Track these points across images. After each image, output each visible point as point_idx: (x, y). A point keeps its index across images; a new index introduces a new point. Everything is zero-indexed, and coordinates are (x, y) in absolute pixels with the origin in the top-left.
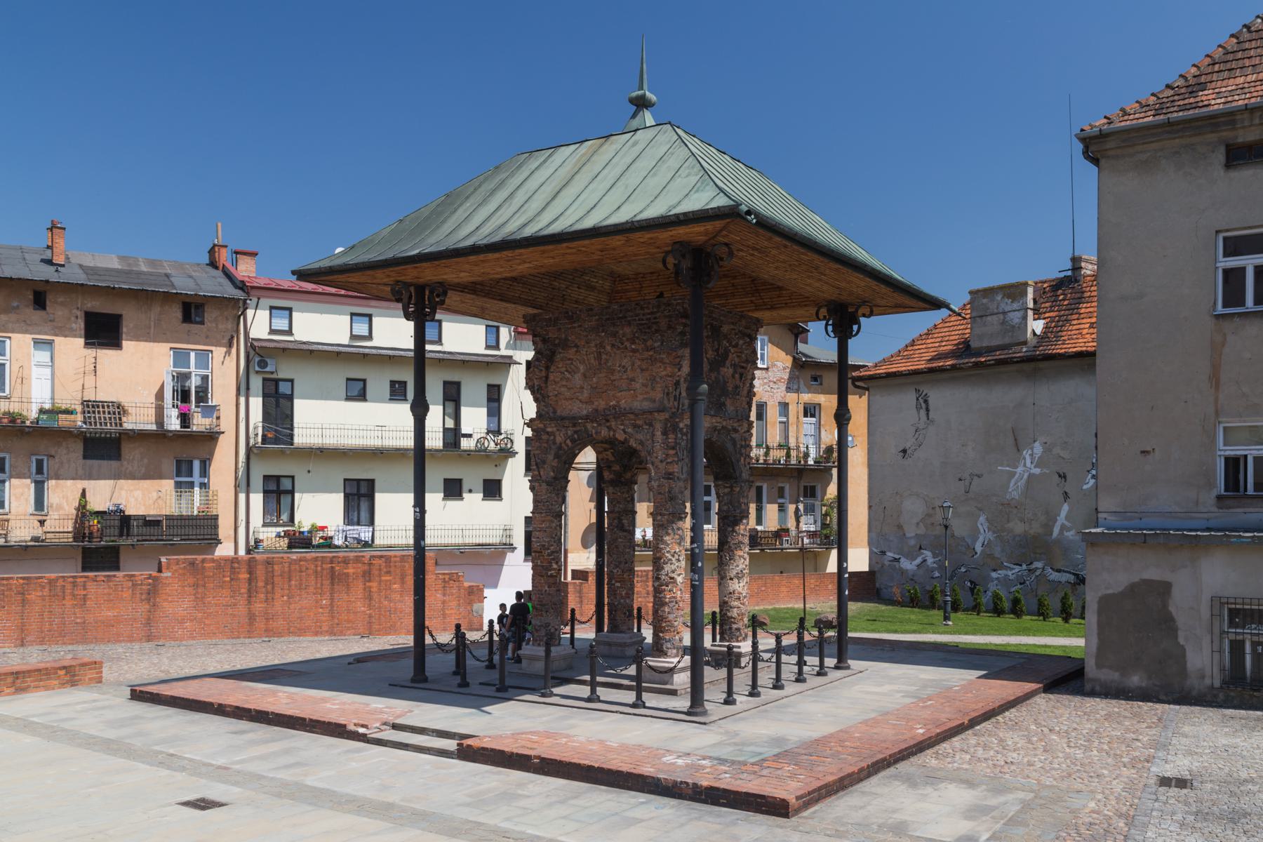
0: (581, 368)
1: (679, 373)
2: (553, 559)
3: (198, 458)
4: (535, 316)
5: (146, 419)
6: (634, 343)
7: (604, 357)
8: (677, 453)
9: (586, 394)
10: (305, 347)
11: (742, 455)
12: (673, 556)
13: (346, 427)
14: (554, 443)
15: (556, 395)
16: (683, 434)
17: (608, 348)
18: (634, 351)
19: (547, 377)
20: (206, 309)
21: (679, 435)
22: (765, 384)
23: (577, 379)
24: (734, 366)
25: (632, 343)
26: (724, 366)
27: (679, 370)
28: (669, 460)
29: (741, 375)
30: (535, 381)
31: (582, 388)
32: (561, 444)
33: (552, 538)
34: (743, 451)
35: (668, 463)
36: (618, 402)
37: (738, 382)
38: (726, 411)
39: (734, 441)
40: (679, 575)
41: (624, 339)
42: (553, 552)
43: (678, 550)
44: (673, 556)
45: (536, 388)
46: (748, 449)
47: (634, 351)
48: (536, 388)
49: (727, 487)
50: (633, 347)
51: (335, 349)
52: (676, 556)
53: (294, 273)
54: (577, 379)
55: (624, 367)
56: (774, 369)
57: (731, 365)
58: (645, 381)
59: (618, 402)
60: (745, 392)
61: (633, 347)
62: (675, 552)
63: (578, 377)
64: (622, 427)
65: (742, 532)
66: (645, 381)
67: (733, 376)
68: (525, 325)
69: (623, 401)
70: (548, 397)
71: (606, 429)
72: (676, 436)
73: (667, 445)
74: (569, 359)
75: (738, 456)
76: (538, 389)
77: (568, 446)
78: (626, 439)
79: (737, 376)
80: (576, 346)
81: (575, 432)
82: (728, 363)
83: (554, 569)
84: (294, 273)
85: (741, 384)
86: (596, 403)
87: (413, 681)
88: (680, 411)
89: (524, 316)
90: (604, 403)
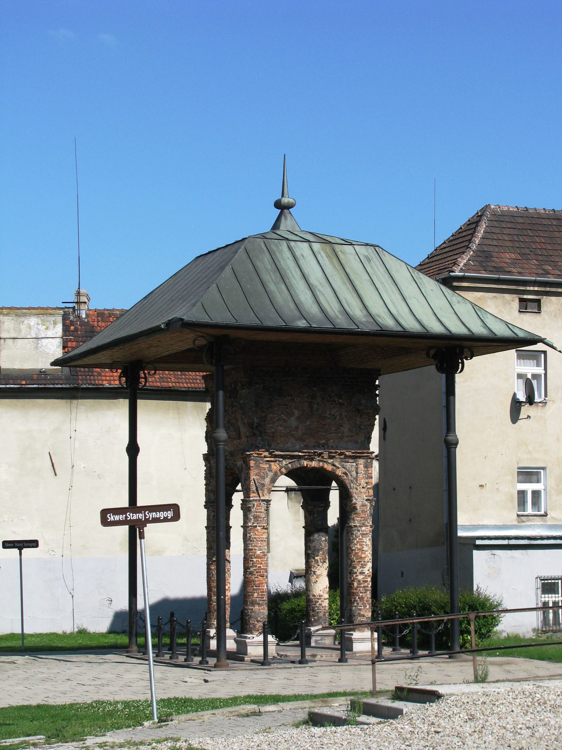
0: (296, 412)
9: (300, 433)
14: (270, 470)
15: (273, 432)
19: (266, 417)
23: (293, 422)
28: (369, 487)
30: (255, 419)
31: (297, 428)
35: (368, 488)
41: (332, 394)
45: (255, 425)
47: (341, 404)
48: (255, 425)
49: (321, 507)
50: (341, 401)
54: (293, 422)
55: (333, 415)
58: (351, 427)
61: (341, 401)
63: (293, 419)
66: (351, 427)
69: (332, 441)
70: (266, 433)
73: (368, 476)
74: (284, 405)
76: (257, 427)
81: (290, 463)
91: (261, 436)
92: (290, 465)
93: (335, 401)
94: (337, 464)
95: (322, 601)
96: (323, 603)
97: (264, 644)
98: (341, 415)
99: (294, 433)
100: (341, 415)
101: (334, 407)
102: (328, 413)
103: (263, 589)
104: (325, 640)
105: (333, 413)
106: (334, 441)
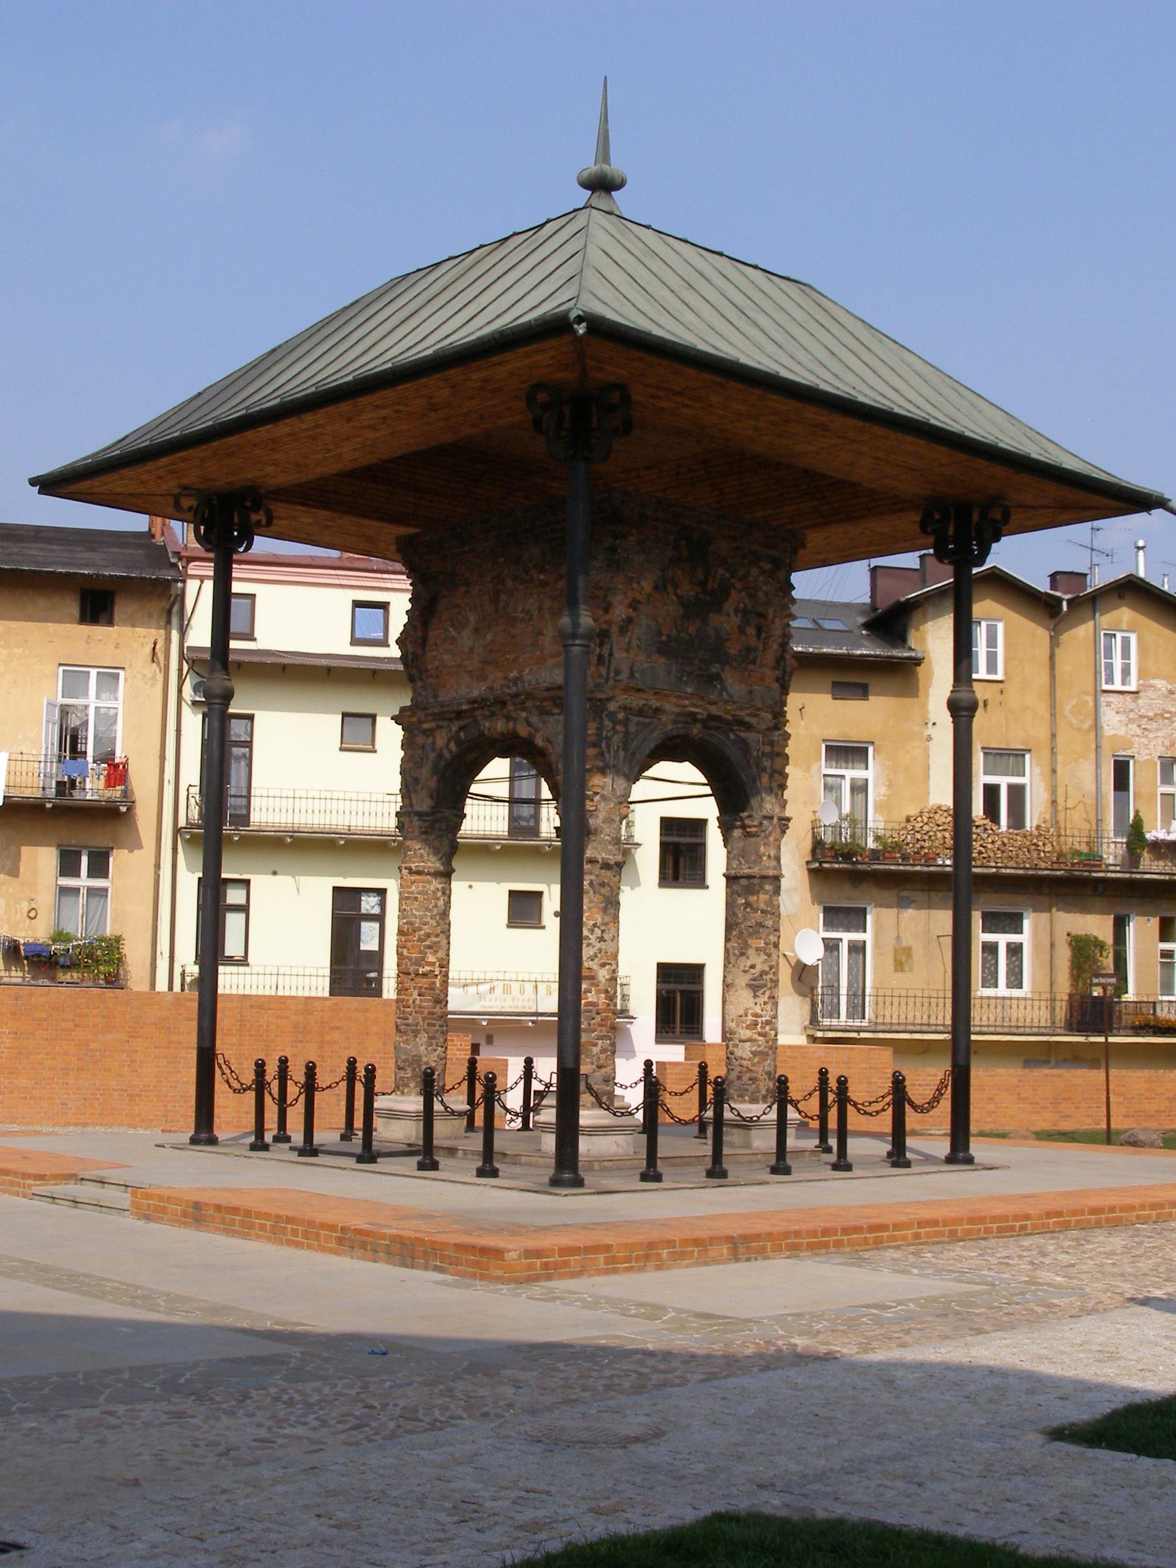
1: (608, 617)
2: (429, 947)
3: (85, 847)
4: (411, 538)
5: (18, 780)
6: (543, 571)
7: (503, 597)
8: (602, 754)
10: (269, 660)
11: (764, 770)
12: (592, 931)
13: (335, 796)
14: (434, 749)
15: (437, 668)
16: (615, 722)
17: (509, 583)
18: (543, 584)
20: (117, 600)
21: (607, 722)
22: (1131, 721)
23: (466, 639)
24: (745, 613)
25: (540, 572)
26: (719, 610)
27: (607, 610)
29: (759, 630)
31: (471, 650)
32: (441, 750)
33: (427, 909)
34: (767, 763)
36: (520, 672)
37: (753, 641)
38: (724, 688)
39: (744, 746)
40: (603, 965)
41: (530, 565)
42: (428, 936)
43: (599, 921)
44: (592, 931)
45: (410, 658)
46: (778, 760)
50: (542, 577)
51: (324, 662)
52: (598, 932)
53: (33, 482)
55: (528, 612)
56: (1150, 693)
57: (736, 611)
59: (520, 672)
60: (770, 658)
61: (542, 577)
62: (595, 925)
63: (466, 633)
64: (524, 714)
65: (762, 906)
67: (742, 630)
68: (399, 557)
69: (527, 671)
70: (427, 670)
71: (504, 720)
72: (601, 722)
75: (754, 770)
76: (413, 659)
77: (450, 751)
78: (530, 734)
79: (751, 631)
80: (467, 584)
81: (461, 728)
82: (728, 606)
83: (433, 964)
84: (33, 482)
85: (761, 648)
86: (491, 677)
87: (194, 1141)
88: (611, 682)
89: (399, 539)
90: (500, 675)
91: (421, 679)
92: (462, 734)
93: (532, 580)
94: (534, 719)
95: (736, 1046)
96: (735, 1049)
97: (432, 1116)
98: (540, 609)
99: (467, 663)
100: (540, 609)
101: (531, 594)
102: (520, 610)
103: (408, 1000)
104: (733, 1134)
105: (528, 607)
106: (530, 671)
